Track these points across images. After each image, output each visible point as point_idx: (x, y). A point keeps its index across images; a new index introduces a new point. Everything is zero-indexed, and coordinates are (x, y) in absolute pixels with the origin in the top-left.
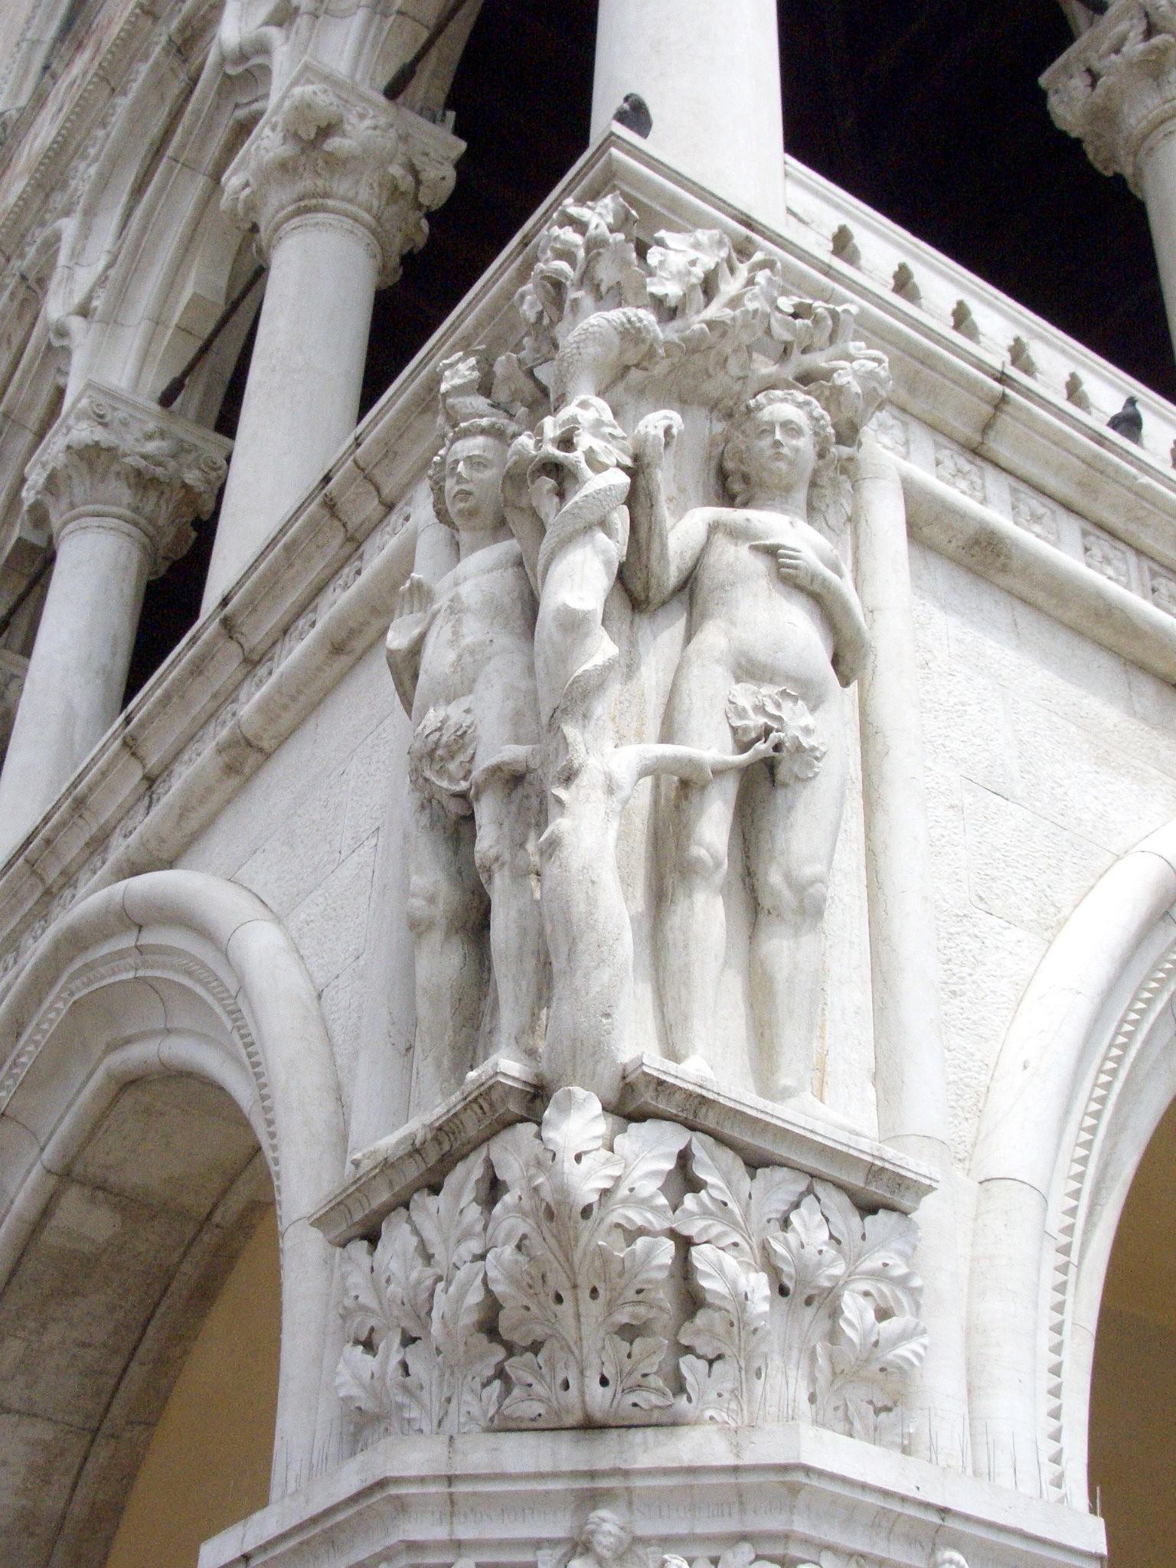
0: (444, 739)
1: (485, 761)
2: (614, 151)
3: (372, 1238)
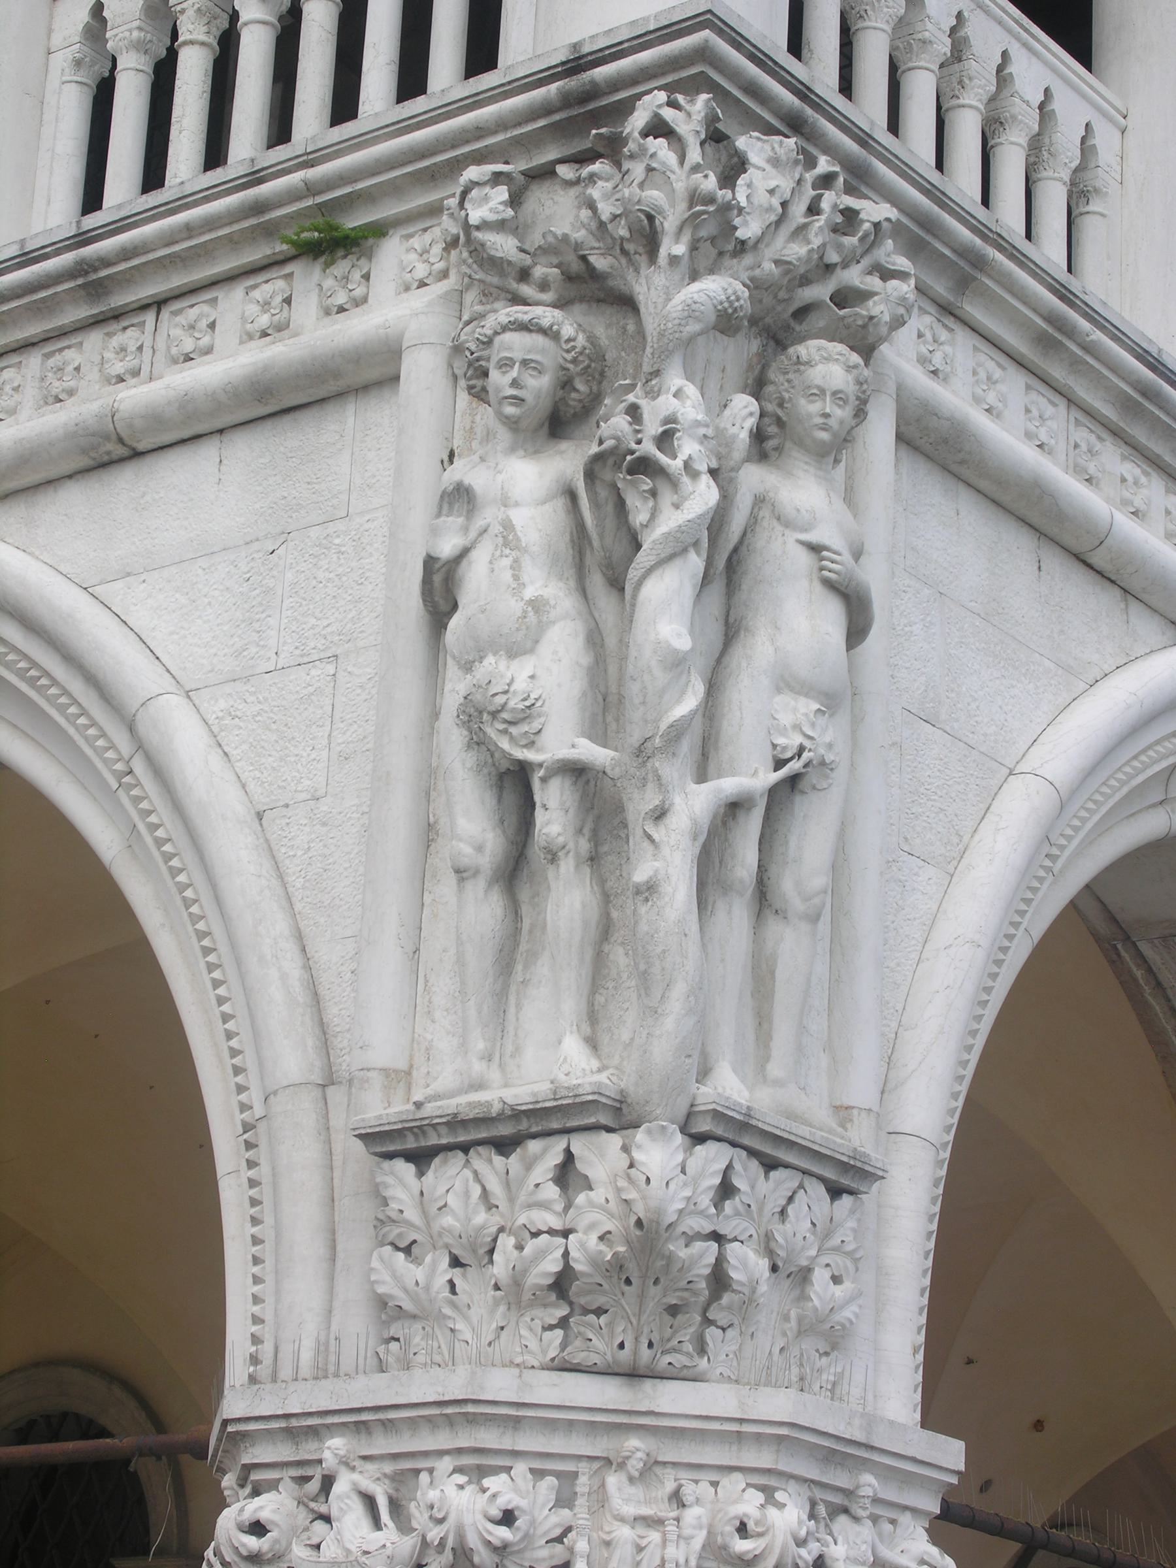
0: (511, 704)
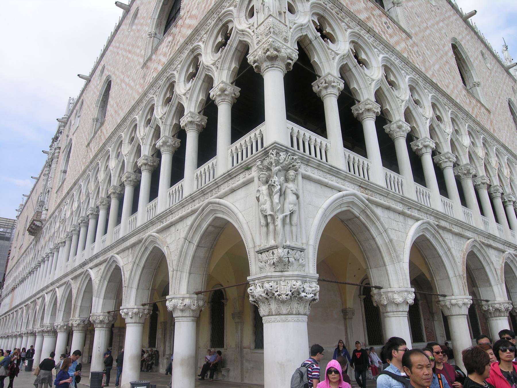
3: (261, 253)
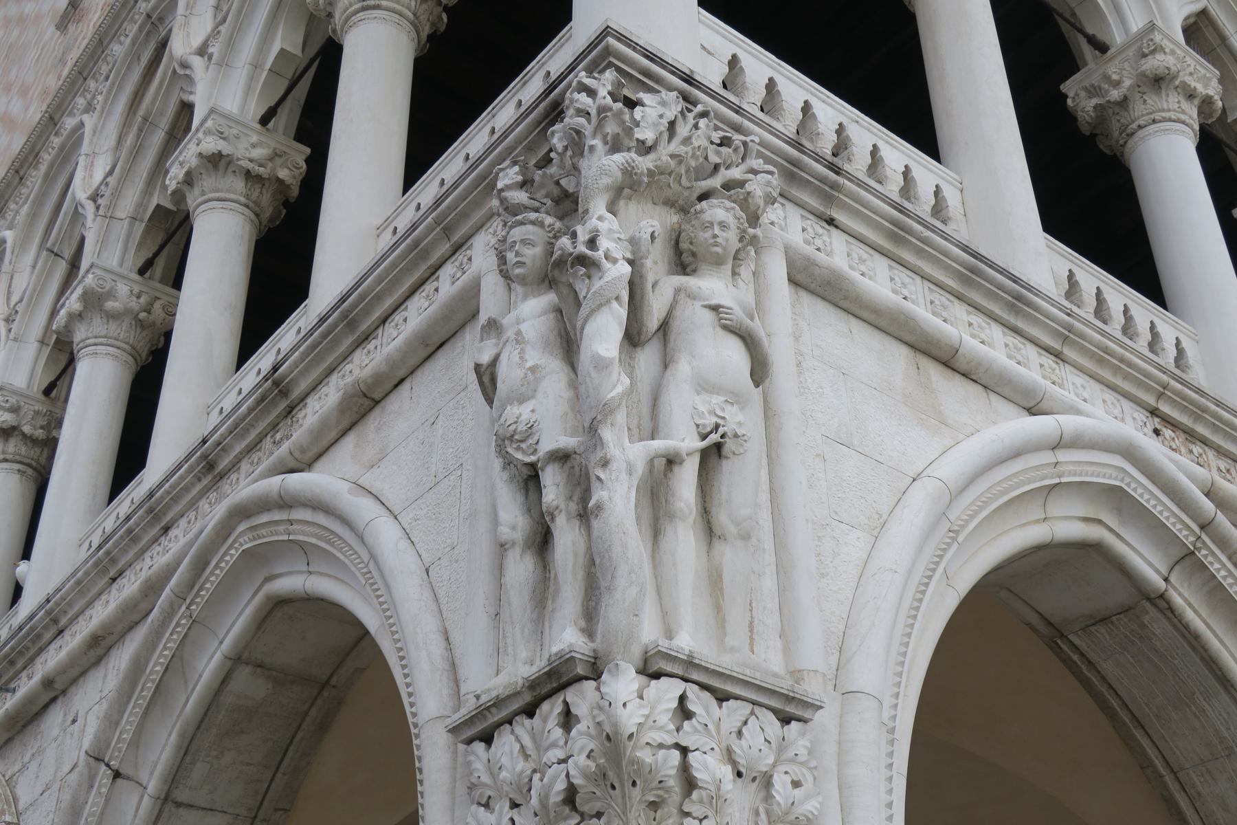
1: (546, 446)
2: (610, 40)
3: (487, 738)
